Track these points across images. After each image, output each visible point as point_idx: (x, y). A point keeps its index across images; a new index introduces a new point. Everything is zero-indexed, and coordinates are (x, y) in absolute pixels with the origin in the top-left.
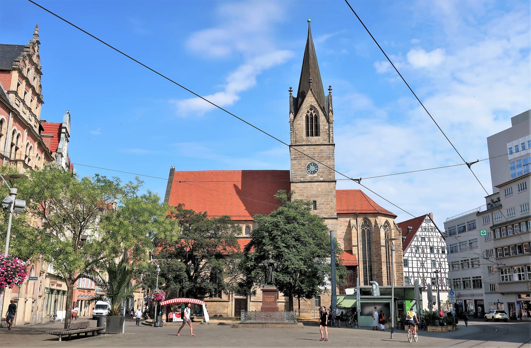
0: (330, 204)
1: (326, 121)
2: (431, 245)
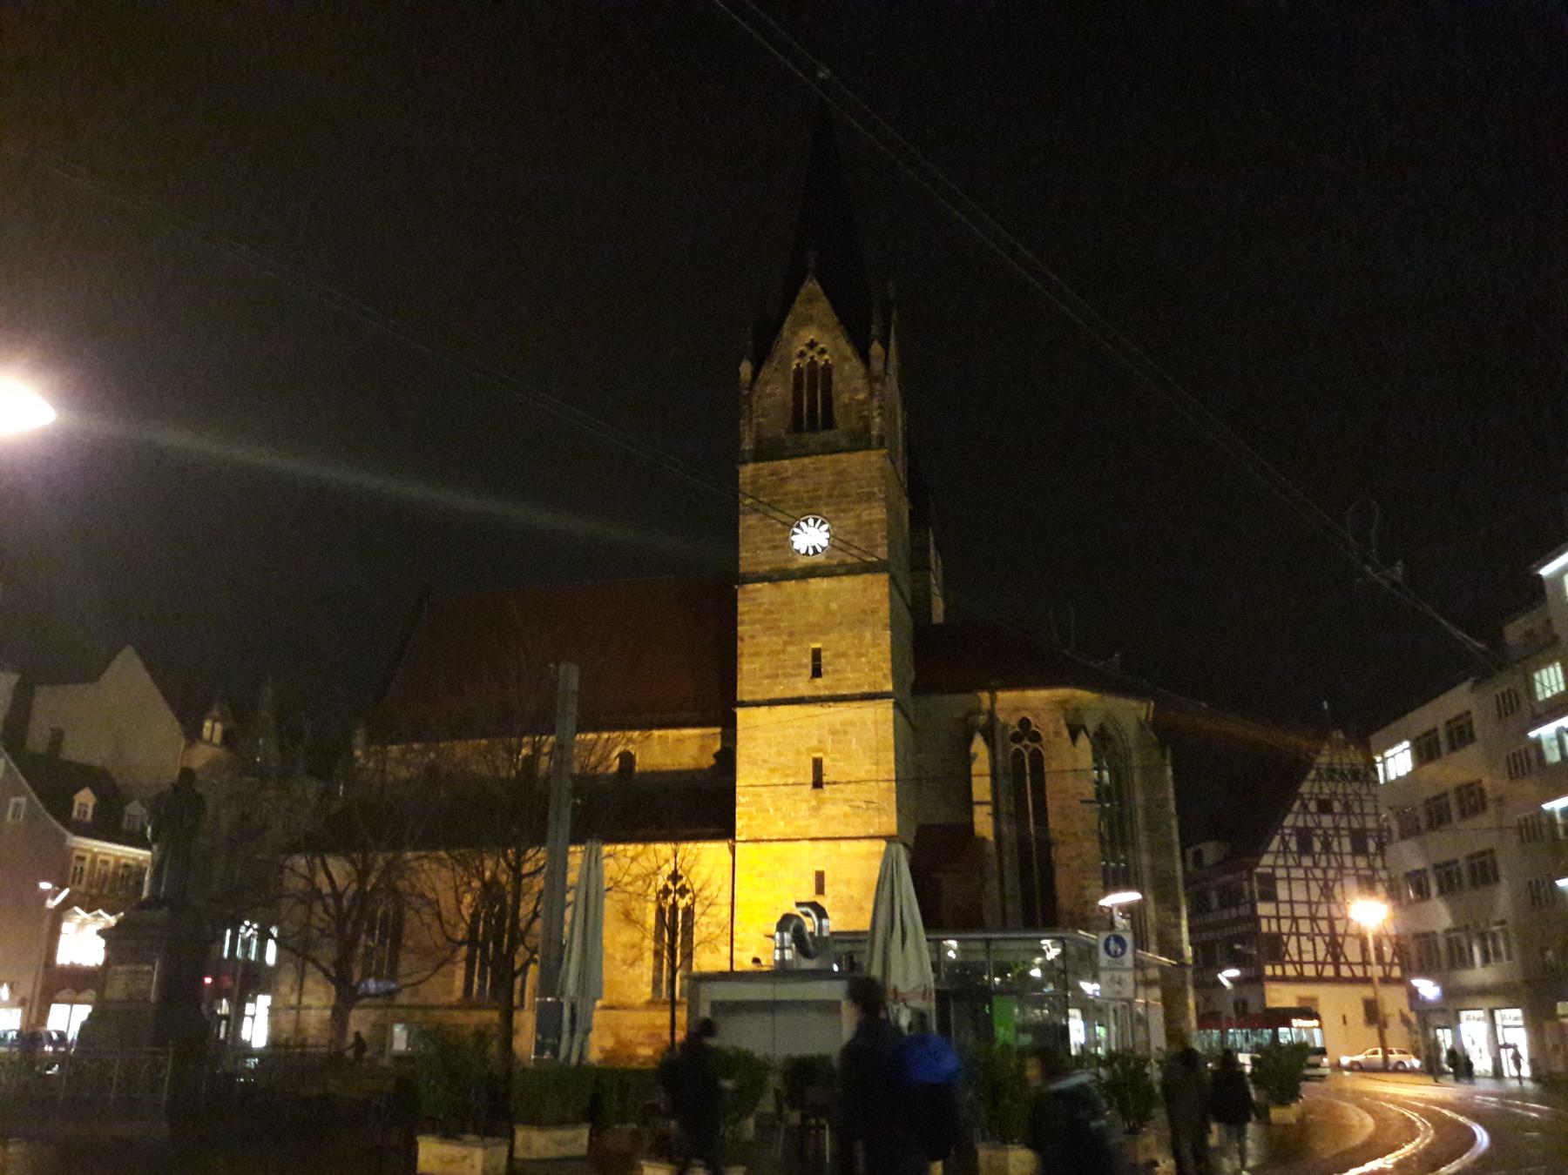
0: (868, 652)
1: (862, 371)
2: (1355, 825)
